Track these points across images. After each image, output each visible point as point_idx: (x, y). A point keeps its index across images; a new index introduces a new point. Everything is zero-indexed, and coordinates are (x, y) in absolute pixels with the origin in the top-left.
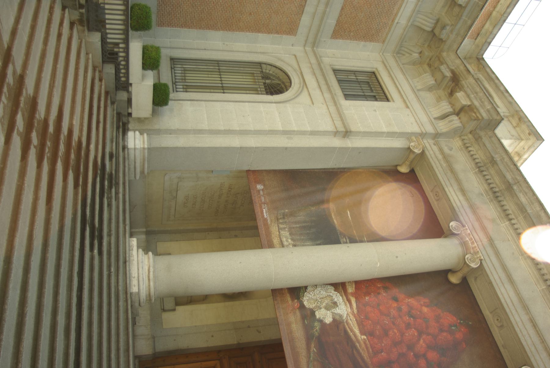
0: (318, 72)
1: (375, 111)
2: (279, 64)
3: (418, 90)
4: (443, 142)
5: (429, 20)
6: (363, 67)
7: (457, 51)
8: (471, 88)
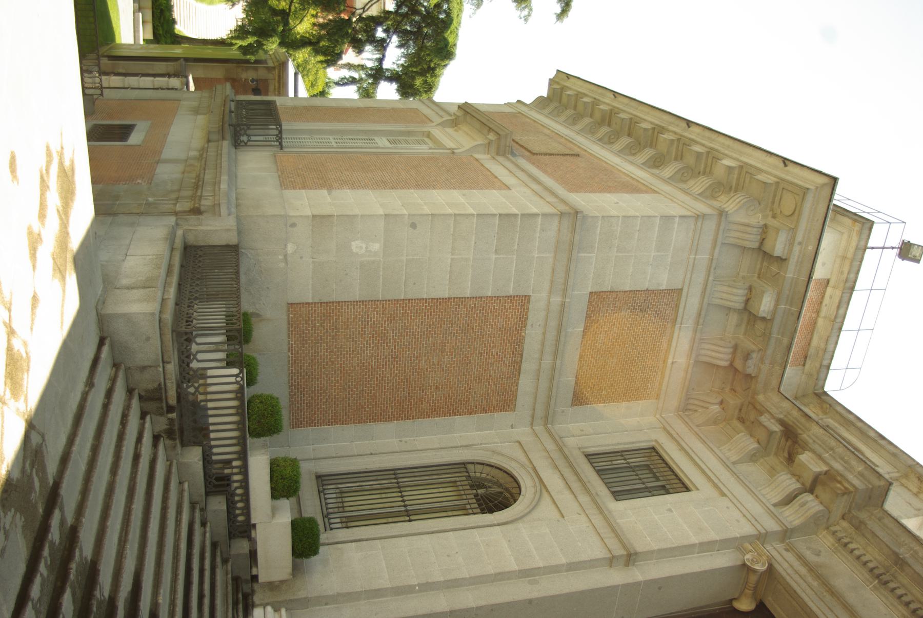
0: (561, 463)
1: (670, 510)
2: (494, 460)
3: (734, 463)
4: (799, 542)
6: (633, 443)
7: (779, 388)
8: (820, 443)
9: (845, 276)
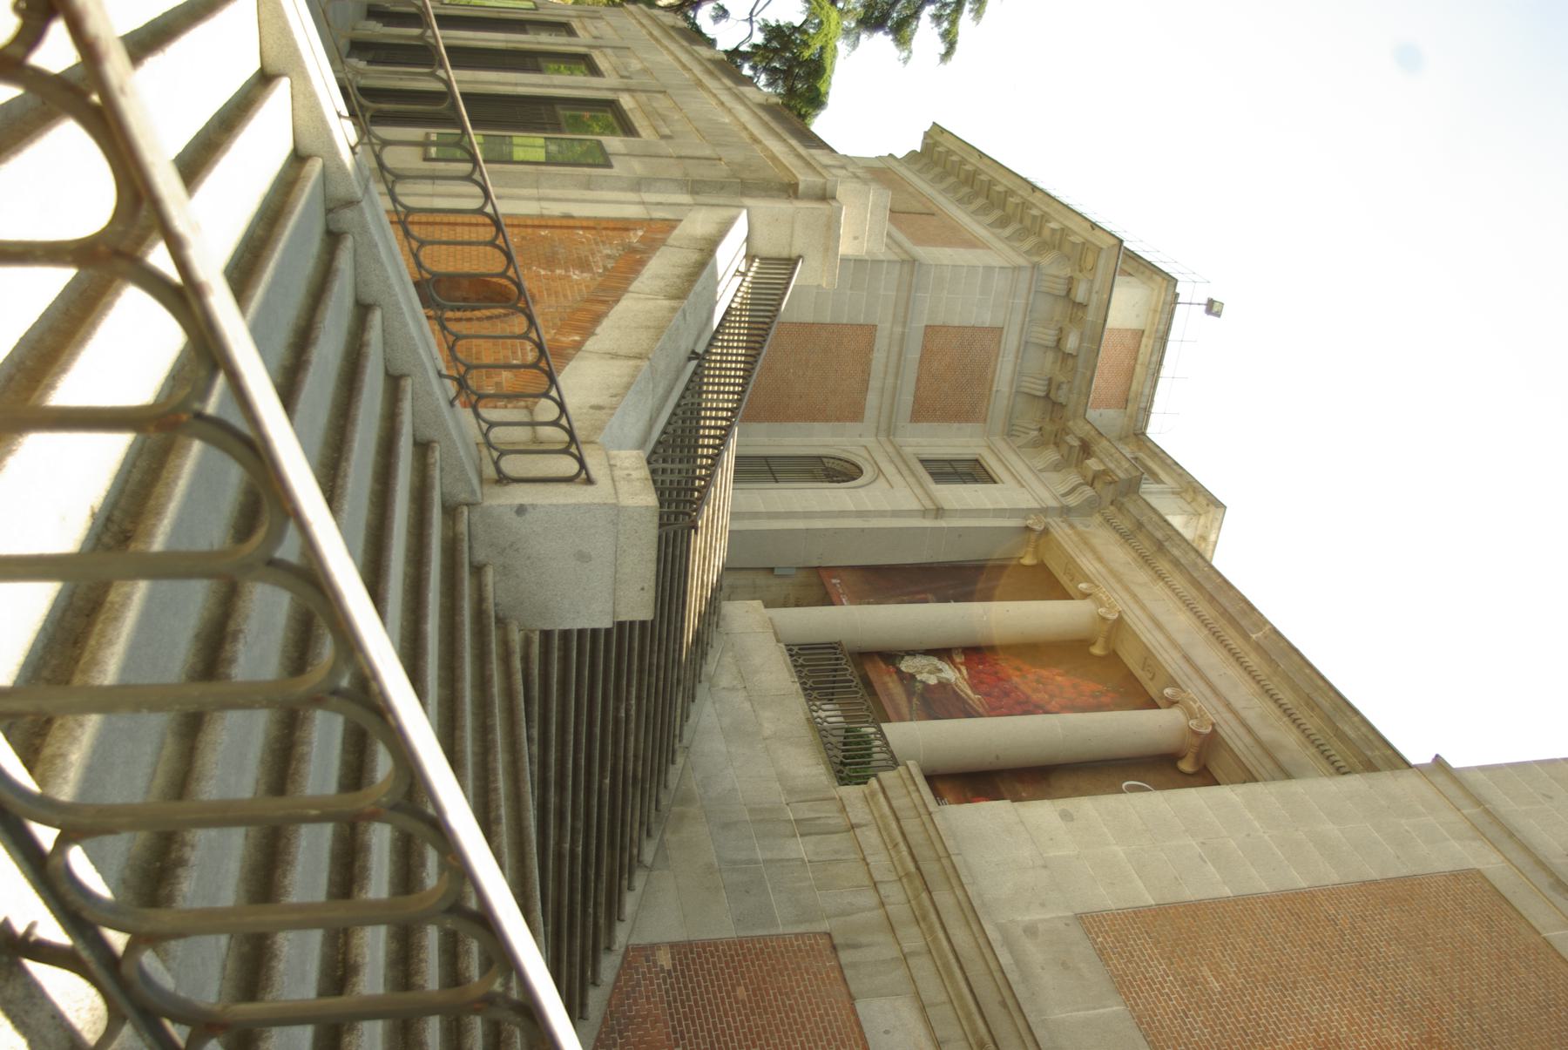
0: (897, 460)
2: (844, 455)
3: (1040, 471)
5: (1038, 381)
7: (1085, 415)
9: (1155, 327)
